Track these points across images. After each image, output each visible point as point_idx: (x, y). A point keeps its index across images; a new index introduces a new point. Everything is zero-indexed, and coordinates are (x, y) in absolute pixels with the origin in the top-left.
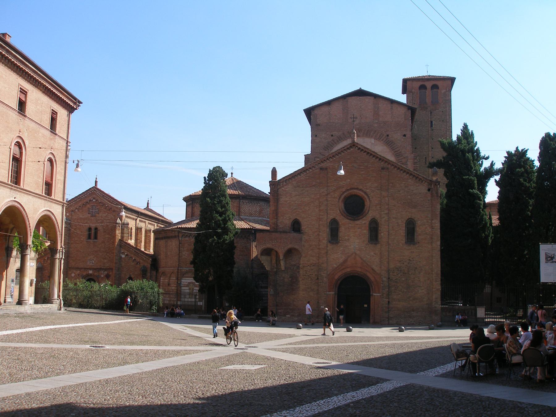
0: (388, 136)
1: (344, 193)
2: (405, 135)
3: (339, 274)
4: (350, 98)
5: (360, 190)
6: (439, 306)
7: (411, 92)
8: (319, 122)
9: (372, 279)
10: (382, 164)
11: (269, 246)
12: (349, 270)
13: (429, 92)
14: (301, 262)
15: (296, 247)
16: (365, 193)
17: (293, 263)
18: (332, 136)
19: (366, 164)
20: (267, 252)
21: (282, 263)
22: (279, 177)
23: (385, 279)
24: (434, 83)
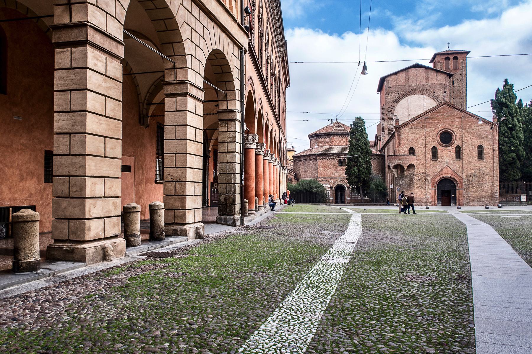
0: (434, 93)
1: (440, 131)
2: (445, 92)
3: (438, 178)
4: (409, 69)
5: (449, 129)
6: (497, 195)
7: (439, 62)
8: (390, 85)
9: (458, 180)
10: (462, 114)
11: (399, 163)
12: (443, 176)
13: (451, 62)
14: (415, 172)
15: (413, 163)
16: (452, 131)
17: (410, 172)
18: (399, 94)
19: (453, 114)
20: (396, 167)
21: (405, 173)
22: (401, 122)
23: (466, 180)
24: (455, 55)
